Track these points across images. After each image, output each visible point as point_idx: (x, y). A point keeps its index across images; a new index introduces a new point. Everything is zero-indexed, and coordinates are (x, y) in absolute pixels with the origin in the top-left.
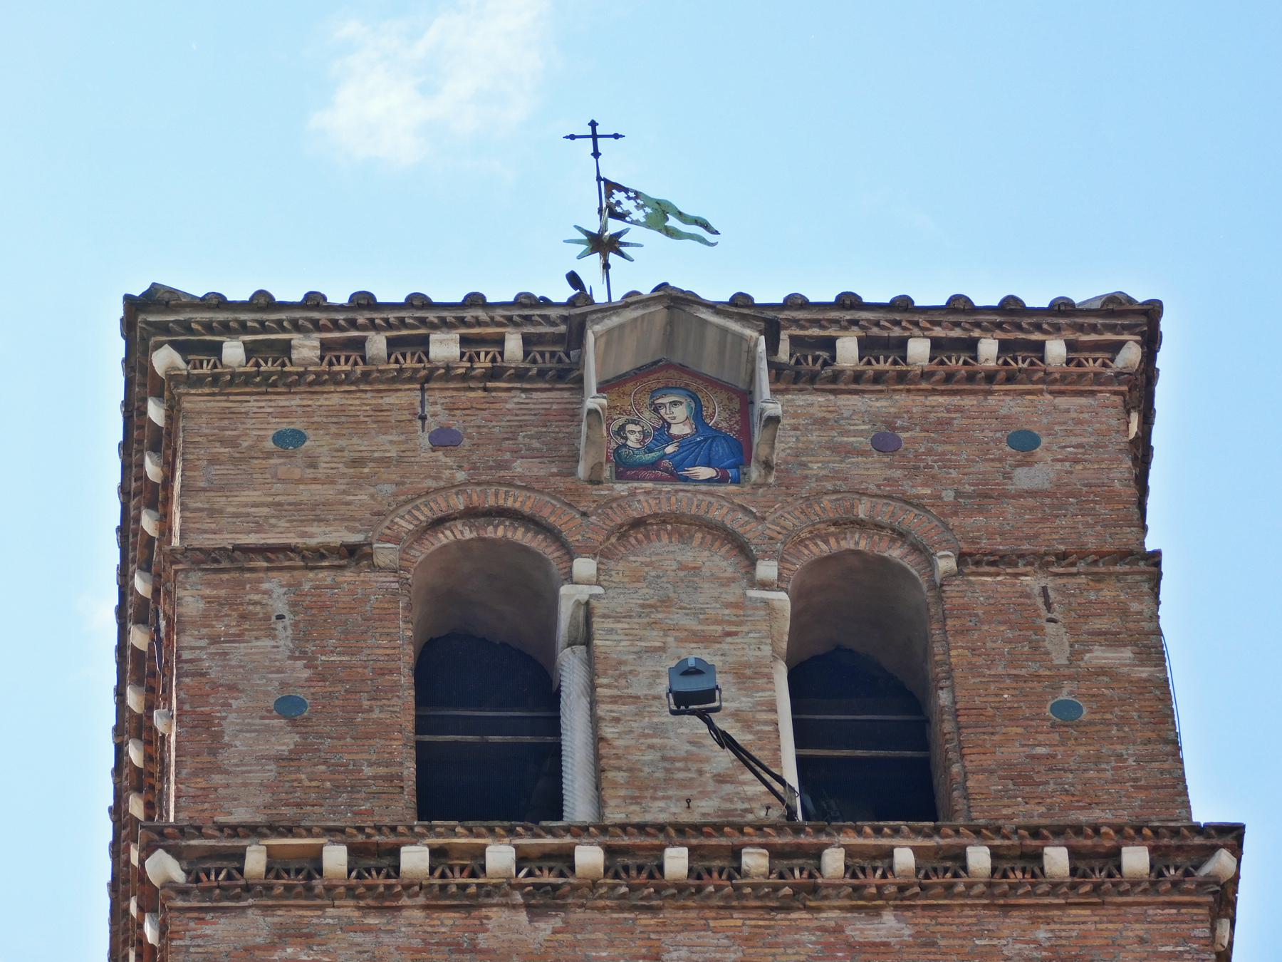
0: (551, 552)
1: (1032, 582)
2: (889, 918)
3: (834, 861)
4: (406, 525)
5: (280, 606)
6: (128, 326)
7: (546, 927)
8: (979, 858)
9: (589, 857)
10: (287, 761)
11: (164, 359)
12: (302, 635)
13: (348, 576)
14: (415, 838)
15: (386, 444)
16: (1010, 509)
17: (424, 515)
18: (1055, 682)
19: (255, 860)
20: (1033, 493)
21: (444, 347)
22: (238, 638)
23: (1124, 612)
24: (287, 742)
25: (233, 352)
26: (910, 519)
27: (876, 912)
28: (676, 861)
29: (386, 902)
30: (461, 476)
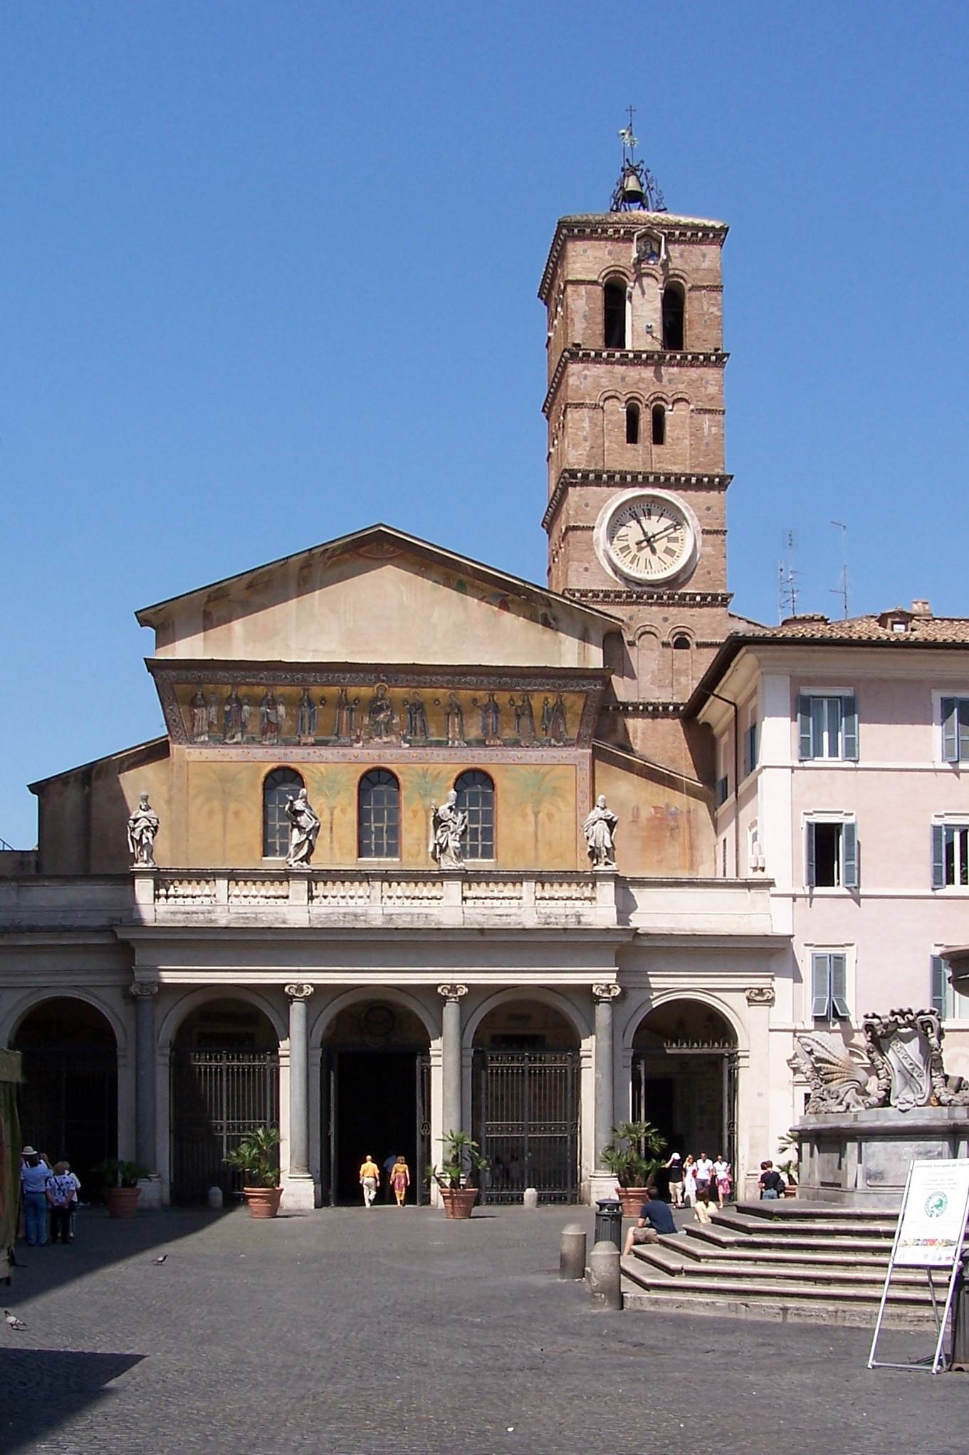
0: (626, 280)
1: (703, 292)
2: (675, 368)
3: (668, 357)
4: (603, 274)
5: (584, 293)
6: (559, 223)
7: (624, 367)
8: (690, 357)
9: (631, 355)
10: (585, 329)
11: (565, 231)
12: (587, 299)
13: (594, 287)
14: (604, 351)
15: (599, 254)
16: (701, 272)
17: (606, 272)
18: (703, 315)
19: (581, 353)
20: (704, 269)
21: (611, 231)
22: (577, 300)
23: (716, 299)
24: (584, 325)
25: (576, 231)
26: (684, 275)
27: (673, 366)
29: (600, 363)
30: (613, 263)
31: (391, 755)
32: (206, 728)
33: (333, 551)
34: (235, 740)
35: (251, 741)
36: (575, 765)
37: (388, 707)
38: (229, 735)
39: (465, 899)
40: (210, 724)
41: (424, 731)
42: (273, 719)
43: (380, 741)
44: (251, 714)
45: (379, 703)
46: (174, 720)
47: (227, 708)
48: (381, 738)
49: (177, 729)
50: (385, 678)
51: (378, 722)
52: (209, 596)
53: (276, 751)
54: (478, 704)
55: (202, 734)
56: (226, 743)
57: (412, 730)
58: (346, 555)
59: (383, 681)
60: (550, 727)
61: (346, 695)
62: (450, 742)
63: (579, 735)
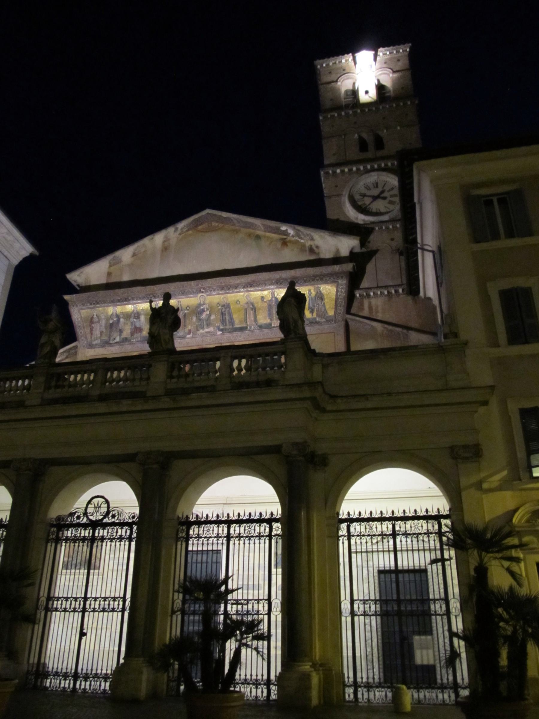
19: (329, 116)
28: (367, 110)
31: (210, 340)
32: (99, 335)
33: (182, 229)
34: (116, 341)
35: (125, 340)
36: (334, 333)
37: (207, 309)
38: (112, 338)
39: (171, 377)
40: (101, 333)
41: (232, 321)
42: (138, 325)
43: (203, 331)
44: (125, 323)
45: (202, 308)
46: (81, 333)
47: (111, 322)
48: (203, 330)
49: (82, 338)
50: (204, 290)
51: (200, 320)
52: (110, 263)
53: (139, 345)
54: (265, 300)
55: (97, 339)
56: (111, 344)
57: (223, 321)
58: (190, 232)
59: (203, 292)
60: (315, 310)
61: (181, 305)
62: (248, 327)
63: (335, 313)
